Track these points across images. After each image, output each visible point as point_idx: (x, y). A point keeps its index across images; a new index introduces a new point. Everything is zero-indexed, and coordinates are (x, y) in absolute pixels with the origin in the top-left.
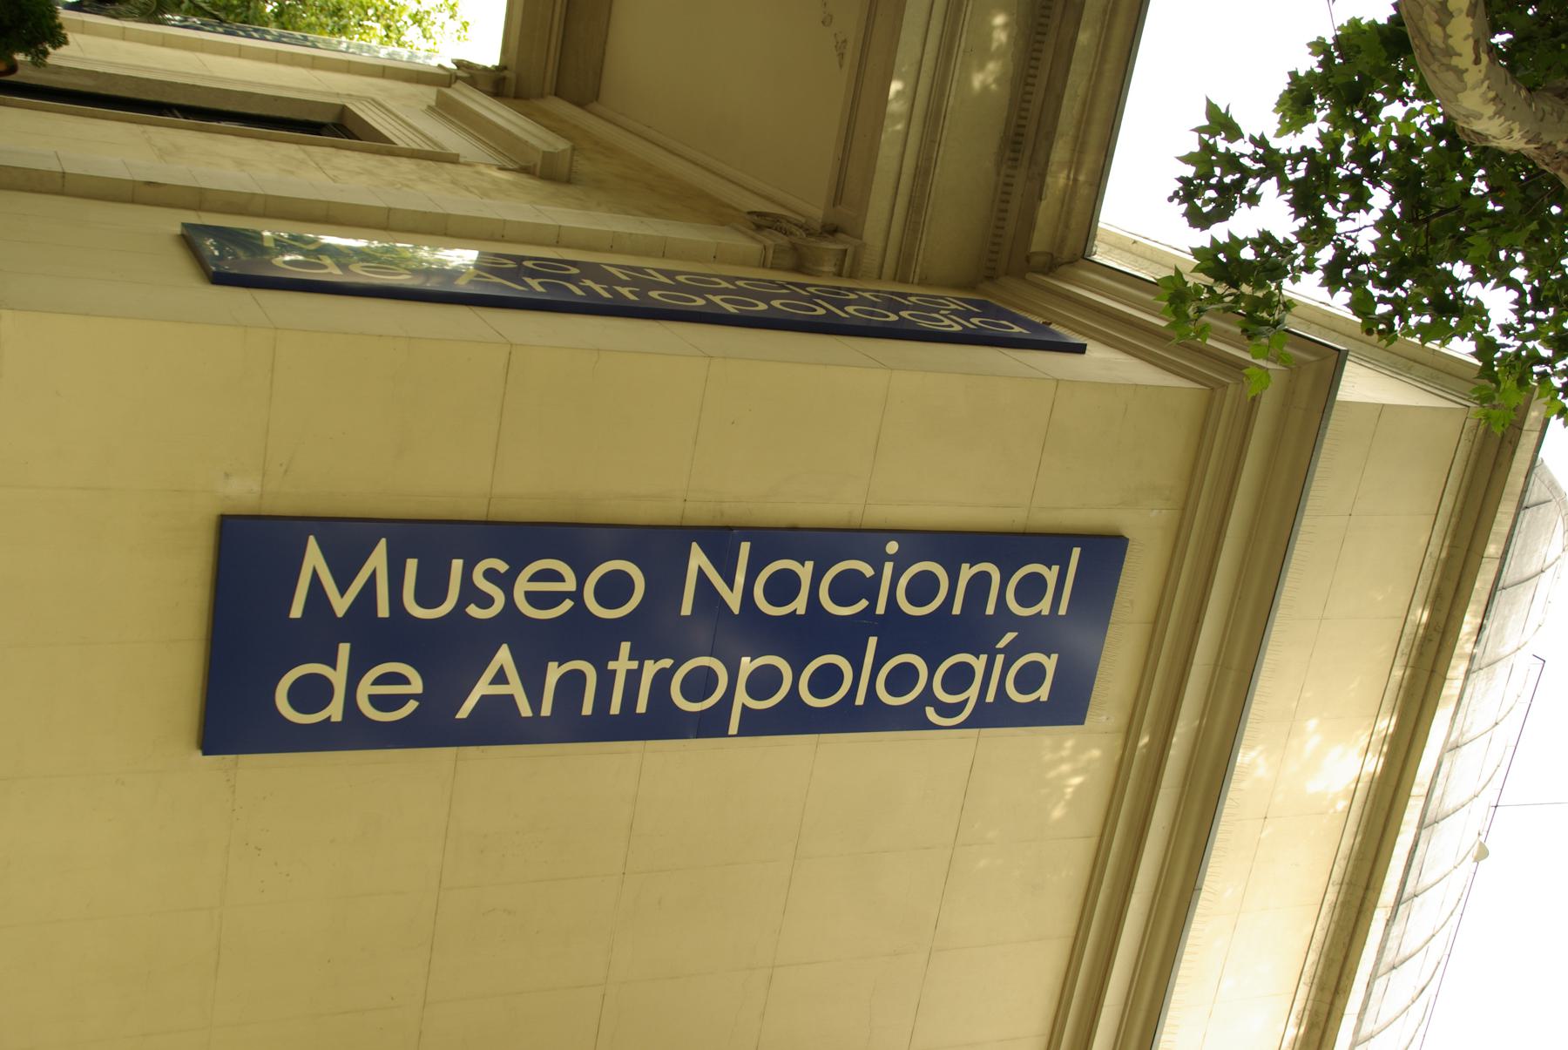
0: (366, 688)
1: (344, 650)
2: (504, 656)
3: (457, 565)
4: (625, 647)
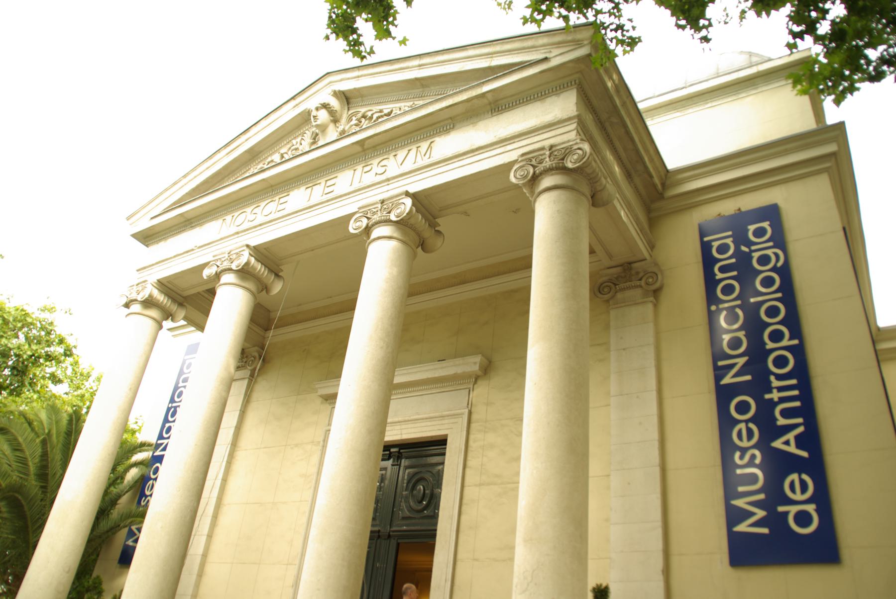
0: (798, 497)
1: (781, 509)
2: (778, 444)
3: (739, 471)
4: (767, 396)
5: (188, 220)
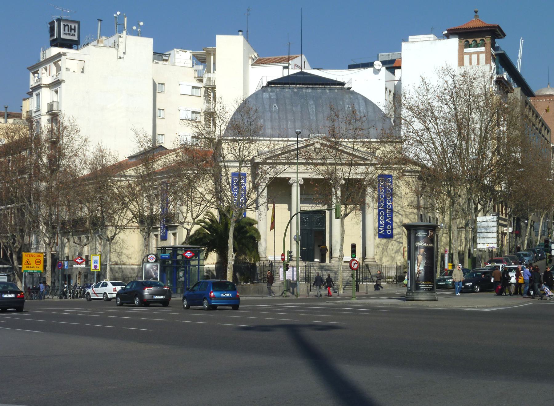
2: (387, 220)
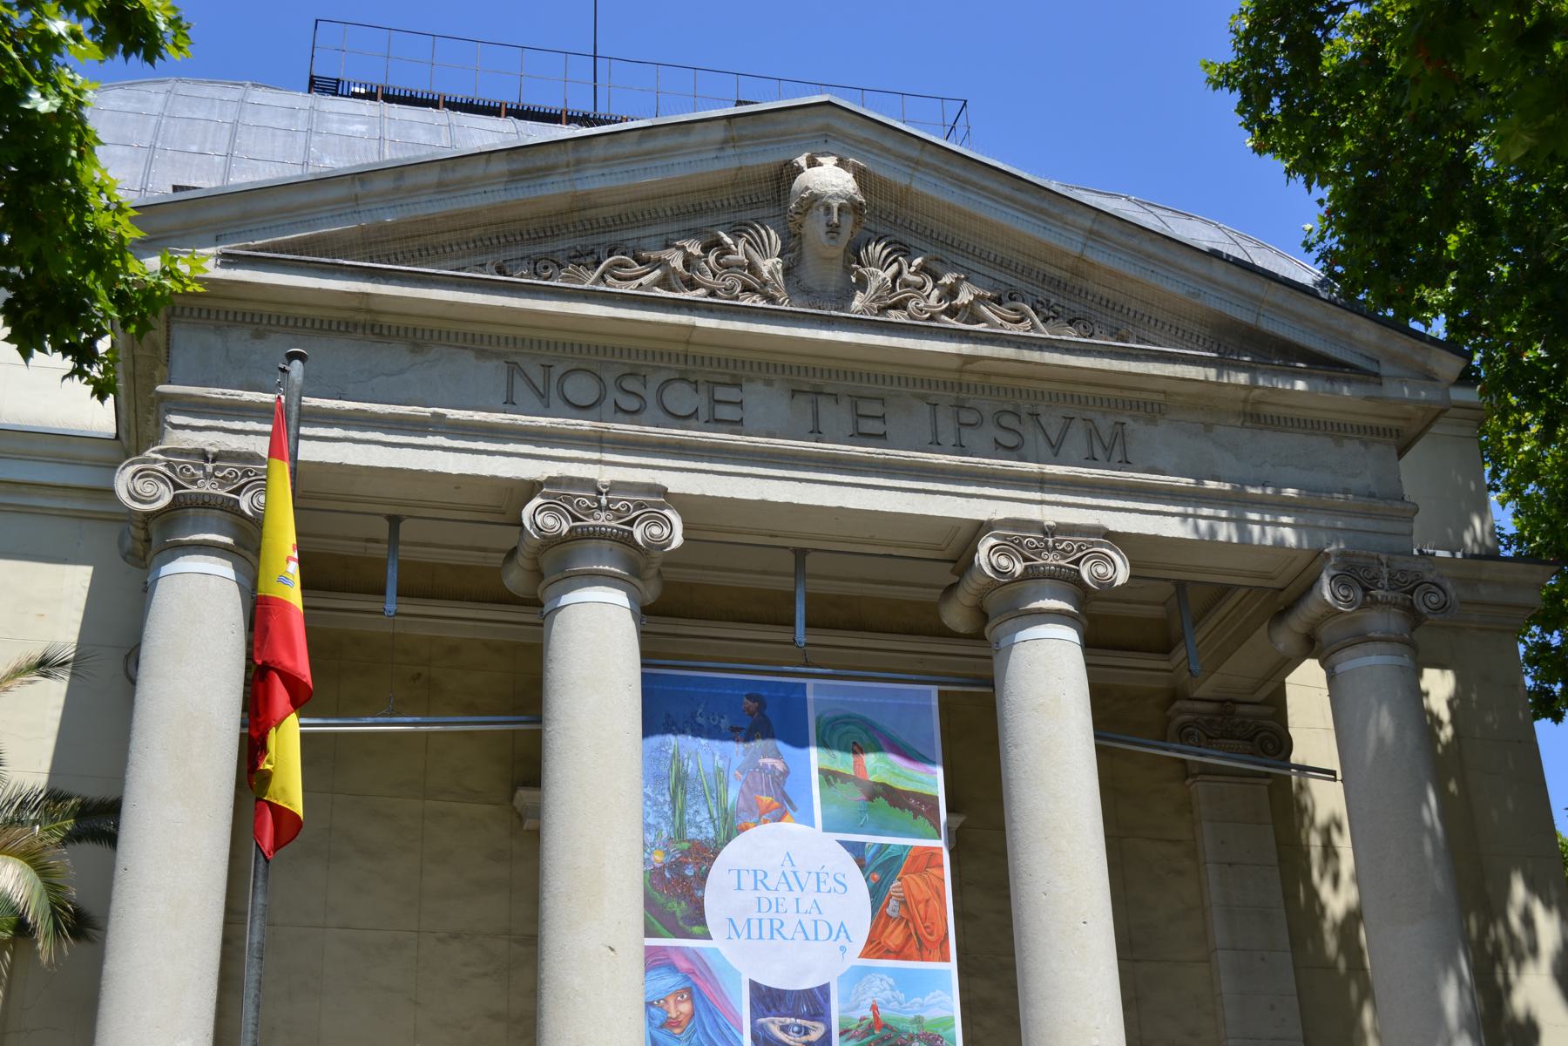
5: (369, 311)
